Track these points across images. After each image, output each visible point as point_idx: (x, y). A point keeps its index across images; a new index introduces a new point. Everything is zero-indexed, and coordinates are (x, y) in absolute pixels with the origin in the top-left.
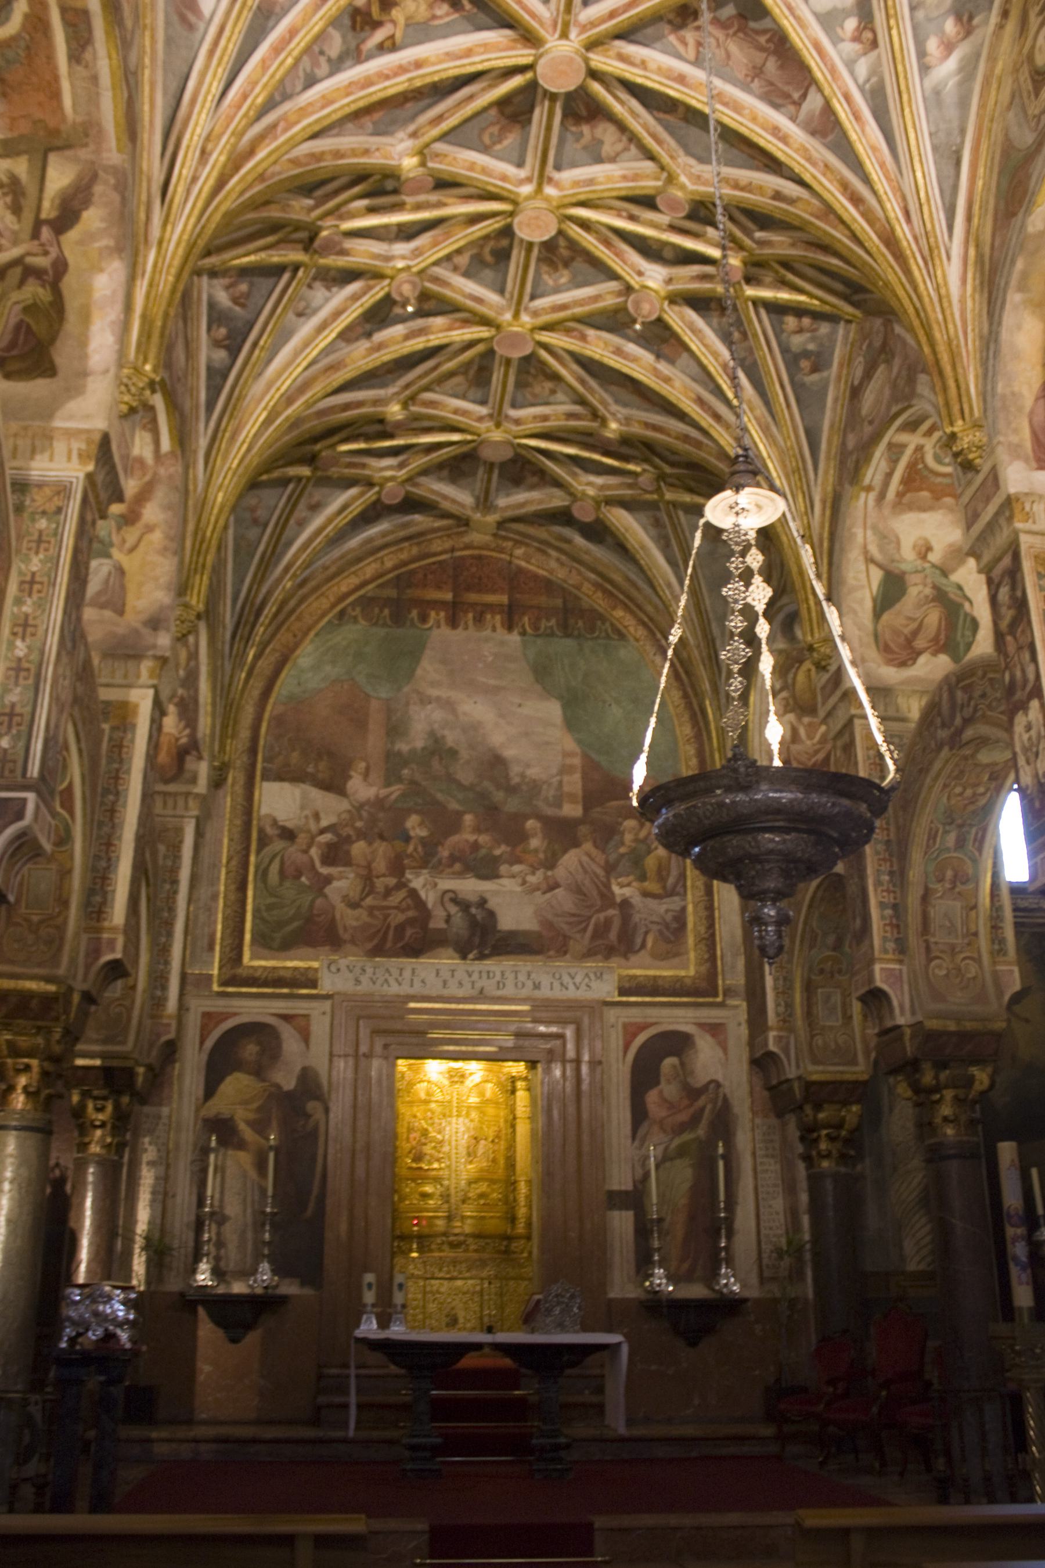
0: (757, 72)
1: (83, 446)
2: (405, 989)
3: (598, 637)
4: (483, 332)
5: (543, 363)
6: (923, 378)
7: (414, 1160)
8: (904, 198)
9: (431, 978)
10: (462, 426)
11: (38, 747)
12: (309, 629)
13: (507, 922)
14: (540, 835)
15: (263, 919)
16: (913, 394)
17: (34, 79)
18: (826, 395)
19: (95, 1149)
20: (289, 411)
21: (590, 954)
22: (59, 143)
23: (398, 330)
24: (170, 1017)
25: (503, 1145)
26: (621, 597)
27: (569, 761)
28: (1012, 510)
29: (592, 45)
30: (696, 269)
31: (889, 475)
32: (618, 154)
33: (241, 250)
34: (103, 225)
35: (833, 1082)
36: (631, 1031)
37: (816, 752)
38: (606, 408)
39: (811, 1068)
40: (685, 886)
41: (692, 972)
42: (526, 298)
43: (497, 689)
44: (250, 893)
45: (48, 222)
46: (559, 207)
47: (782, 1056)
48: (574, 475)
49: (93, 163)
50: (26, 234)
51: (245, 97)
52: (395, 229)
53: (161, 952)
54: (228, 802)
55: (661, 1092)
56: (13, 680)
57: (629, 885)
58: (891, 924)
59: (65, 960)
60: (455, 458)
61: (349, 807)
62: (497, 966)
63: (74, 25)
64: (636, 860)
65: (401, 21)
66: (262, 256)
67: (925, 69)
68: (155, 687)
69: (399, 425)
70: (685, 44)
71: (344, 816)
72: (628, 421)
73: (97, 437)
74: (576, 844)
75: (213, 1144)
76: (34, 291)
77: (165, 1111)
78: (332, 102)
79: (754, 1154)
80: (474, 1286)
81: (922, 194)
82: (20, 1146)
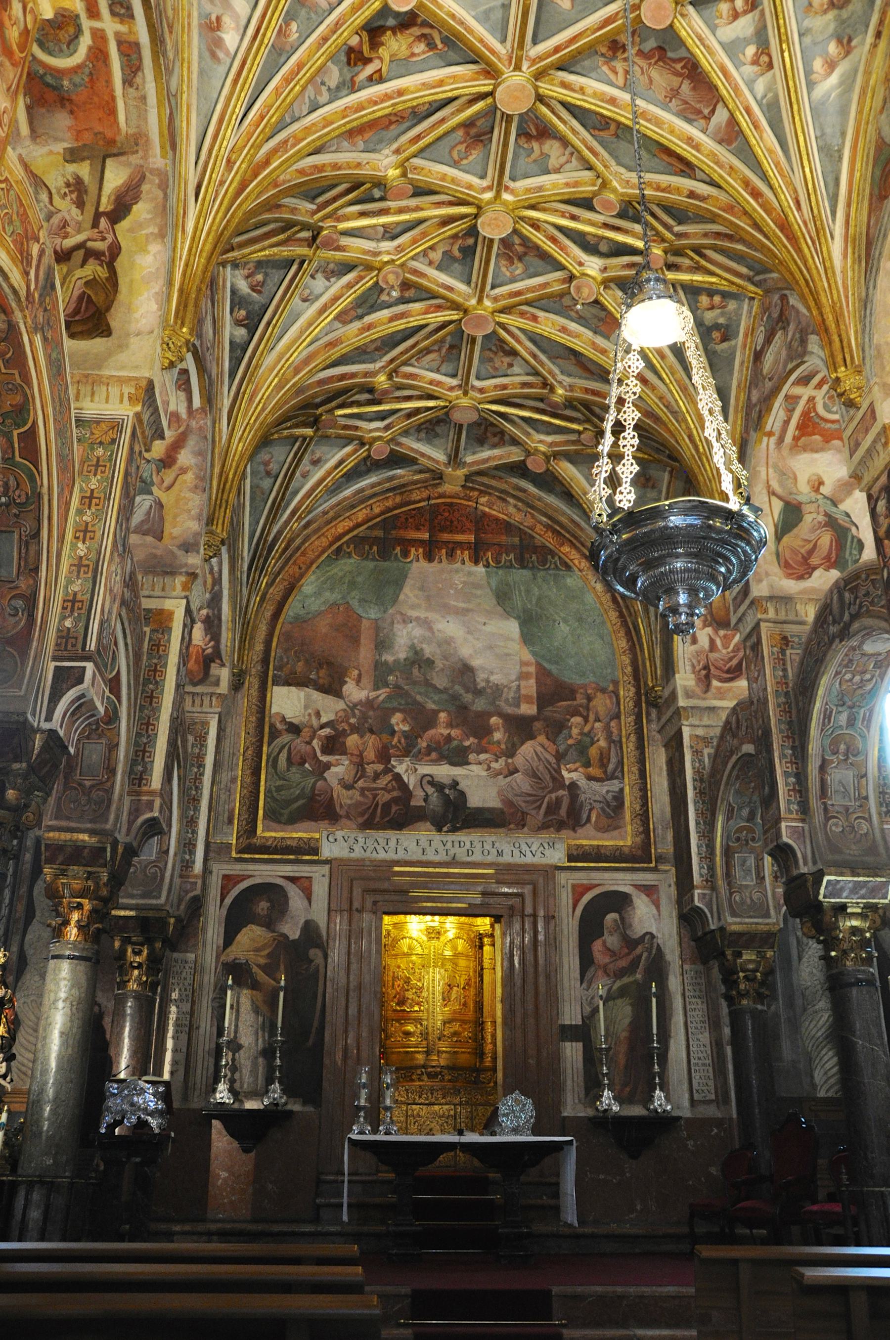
0: (674, 93)
1: (133, 391)
2: (391, 856)
3: (549, 568)
4: (454, 316)
5: (502, 341)
6: (813, 338)
7: (398, 1004)
8: (795, 191)
9: (412, 846)
10: (436, 394)
11: (95, 627)
12: (312, 563)
13: (475, 800)
14: (502, 729)
15: (273, 797)
16: (805, 352)
17: (96, 99)
18: (734, 359)
19: (133, 986)
20: (296, 378)
21: (544, 827)
22: (115, 151)
23: (385, 313)
24: (196, 876)
25: (472, 992)
26: (567, 535)
27: (525, 669)
28: (886, 437)
29: (539, 75)
30: (626, 259)
31: (787, 423)
32: (561, 166)
33: (257, 247)
34: (149, 216)
35: (748, 933)
36: (579, 891)
37: (731, 659)
38: (554, 377)
39: (730, 920)
40: (622, 771)
41: (629, 843)
42: (488, 287)
43: (466, 611)
44: (263, 777)
45: (104, 214)
46: (513, 210)
47: (706, 910)
48: (528, 434)
49: (142, 166)
50: (89, 225)
51: (262, 118)
52: (382, 229)
53: (190, 823)
54: (245, 702)
55: (604, 942)
56: (86, 506)
57: (576, 770)
58: (794, 790)
59: (112, 817)
60: (430, 421)
61: (345, 707)
62: (465, 837)
63: (129, 55)
64: (582, 749)
65: (387, 58)
66: (275, 250)
67: (811, 85)
68: (186, 597)
69: (385, 392)
70: (616, 73)
71: (342, 714)
72: (571, 388)
73: (144, 384)
74: (532, 737)
75: (230, 982)
76: (93, 269)
77: (191, 956)
78: (332, 123)
79: (684, 995)
80: (449, 1110)
81: (810, 186)
82: (73, 971)
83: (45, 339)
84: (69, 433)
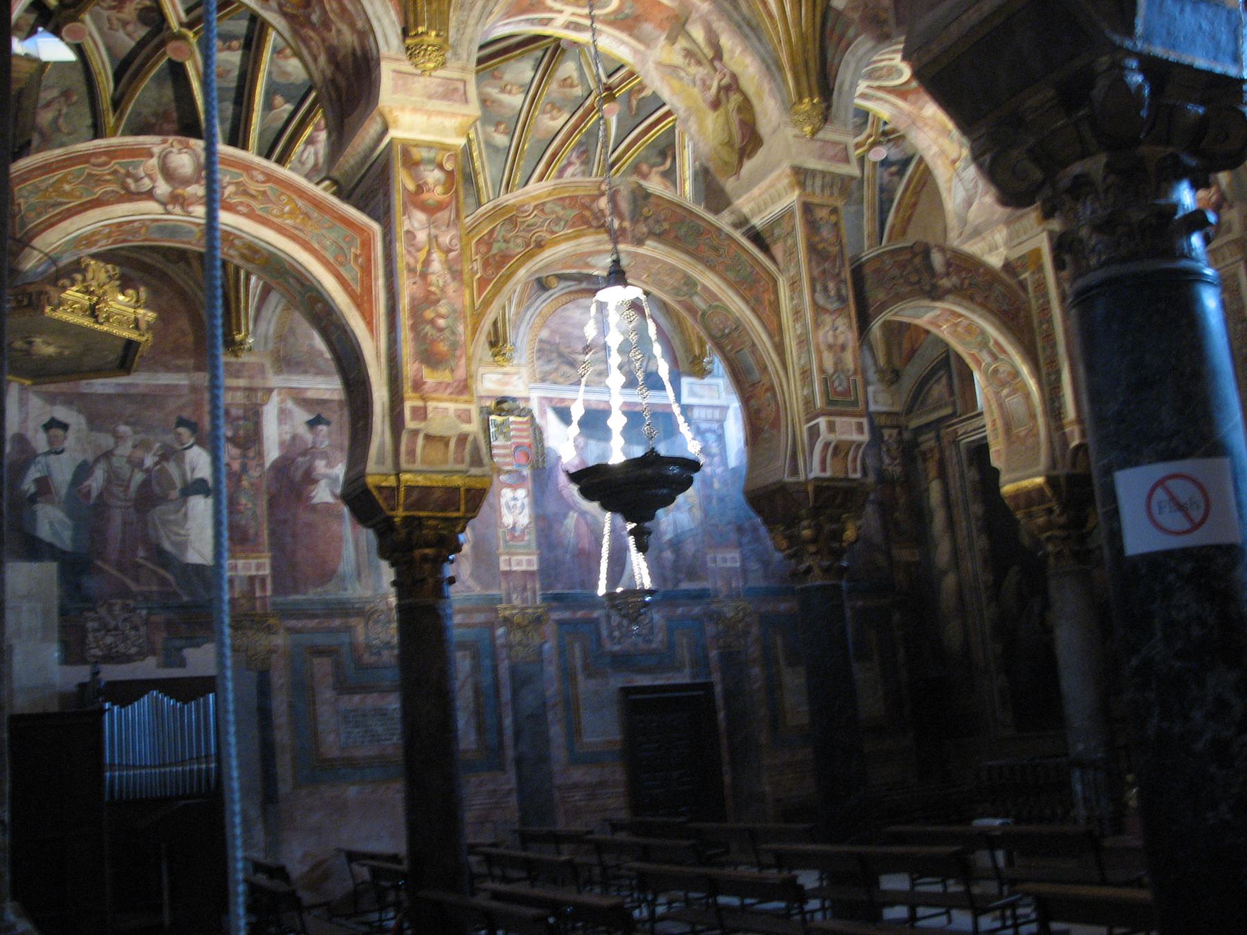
22: (683, 20)
49: (701, 17)
50: (712, 73)
73: (788, 171)
76: (735, 98)
83: (660, 237)
84: (744, 257)
